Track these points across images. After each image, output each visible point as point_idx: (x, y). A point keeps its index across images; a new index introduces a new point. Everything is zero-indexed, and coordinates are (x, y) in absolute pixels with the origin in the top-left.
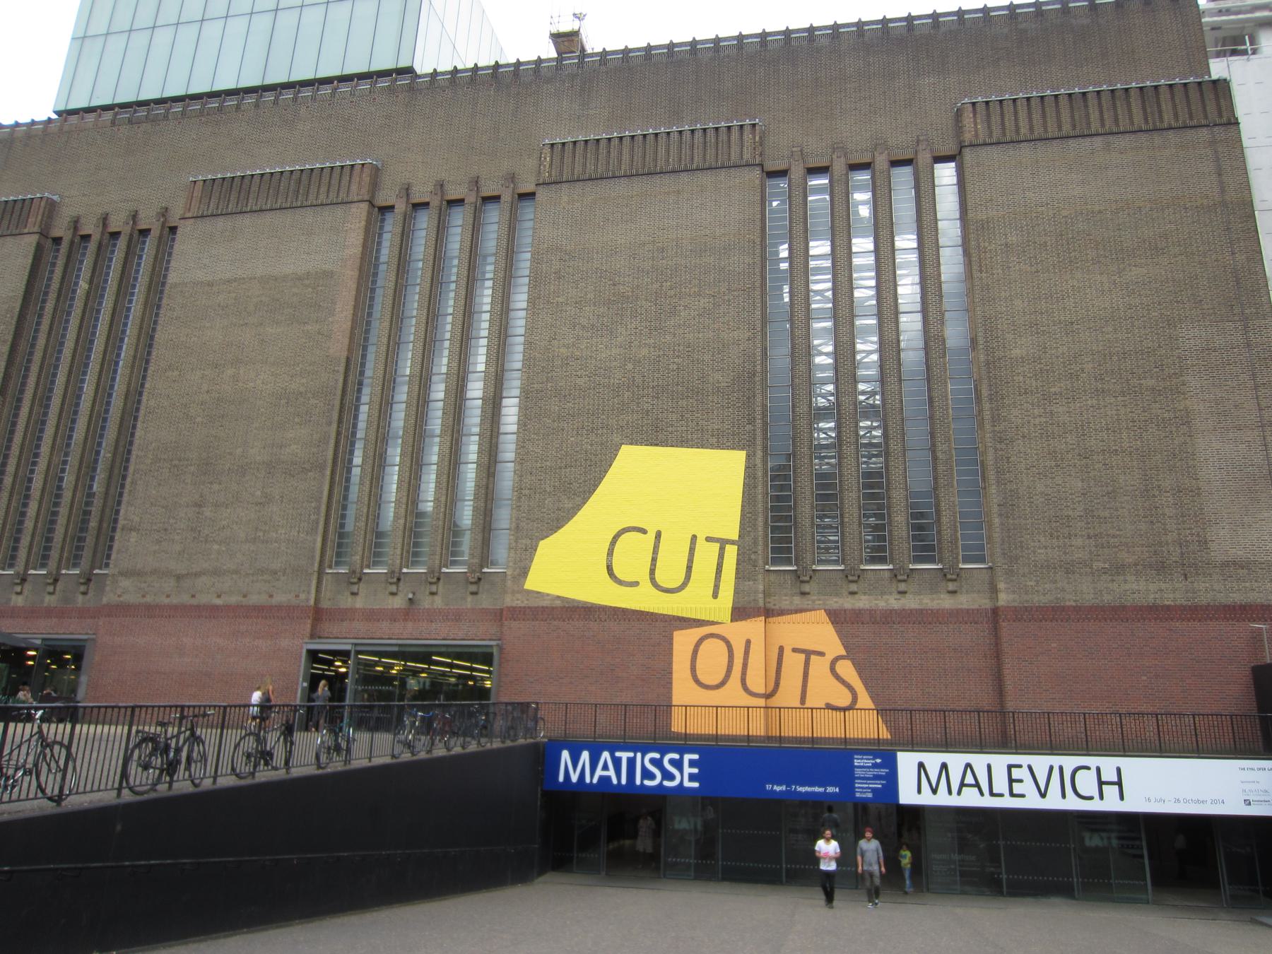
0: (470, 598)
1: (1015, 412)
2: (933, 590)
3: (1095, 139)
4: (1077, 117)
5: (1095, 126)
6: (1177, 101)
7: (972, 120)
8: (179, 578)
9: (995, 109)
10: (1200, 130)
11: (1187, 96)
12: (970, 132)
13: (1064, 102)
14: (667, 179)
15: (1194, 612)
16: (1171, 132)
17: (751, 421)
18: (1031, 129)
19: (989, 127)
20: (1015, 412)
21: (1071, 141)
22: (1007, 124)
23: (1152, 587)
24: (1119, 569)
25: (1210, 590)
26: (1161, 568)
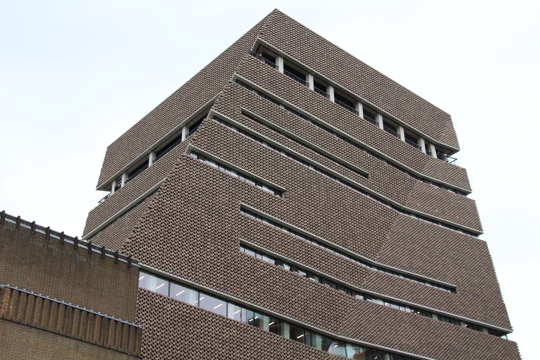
3: (72, 340)
4: (66, 322)
5: (74, 333)
6: (117, 333)
7: (8, 301)
9: (23, 298)
10: (123, 355)
11: (122, 331)
12: (5, 308)
13: (61, 309)
16: (110, 351)
18: (40, 321)
19: (17, 310)
21: (59, 337)
22: (28, 311)
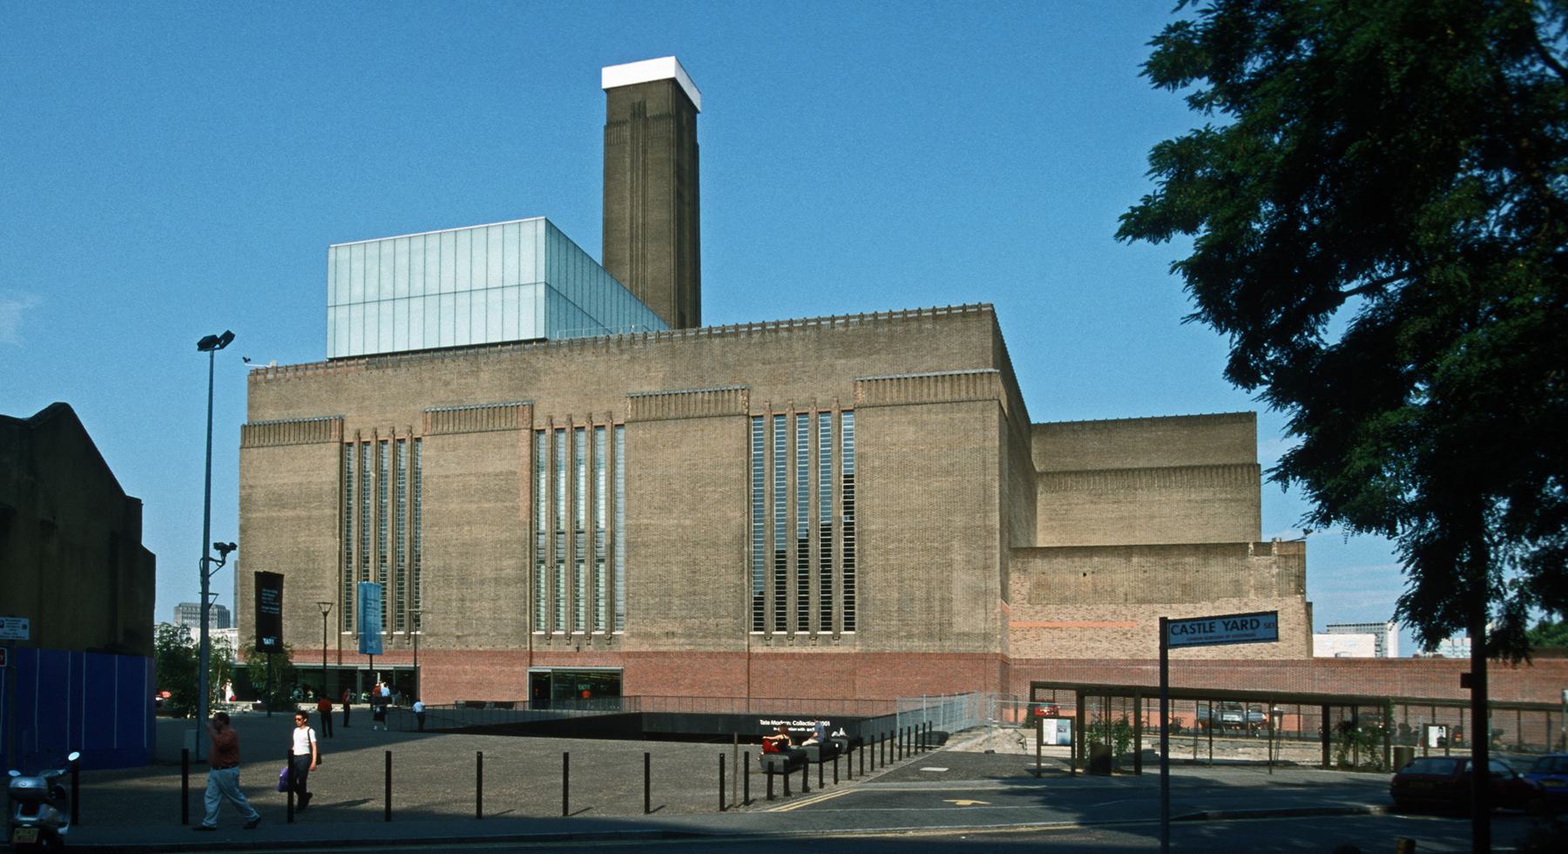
0: (607, 647)
1: (870, 558)
2: (828, 644)
8: (458, 637)
14: (697, 422)
15: (942, 656)
17: (742, 560)
20: (870, 558)
23: (925, 644)
24: (910, 636)
25: (949, 646)
26: (930, 636)
